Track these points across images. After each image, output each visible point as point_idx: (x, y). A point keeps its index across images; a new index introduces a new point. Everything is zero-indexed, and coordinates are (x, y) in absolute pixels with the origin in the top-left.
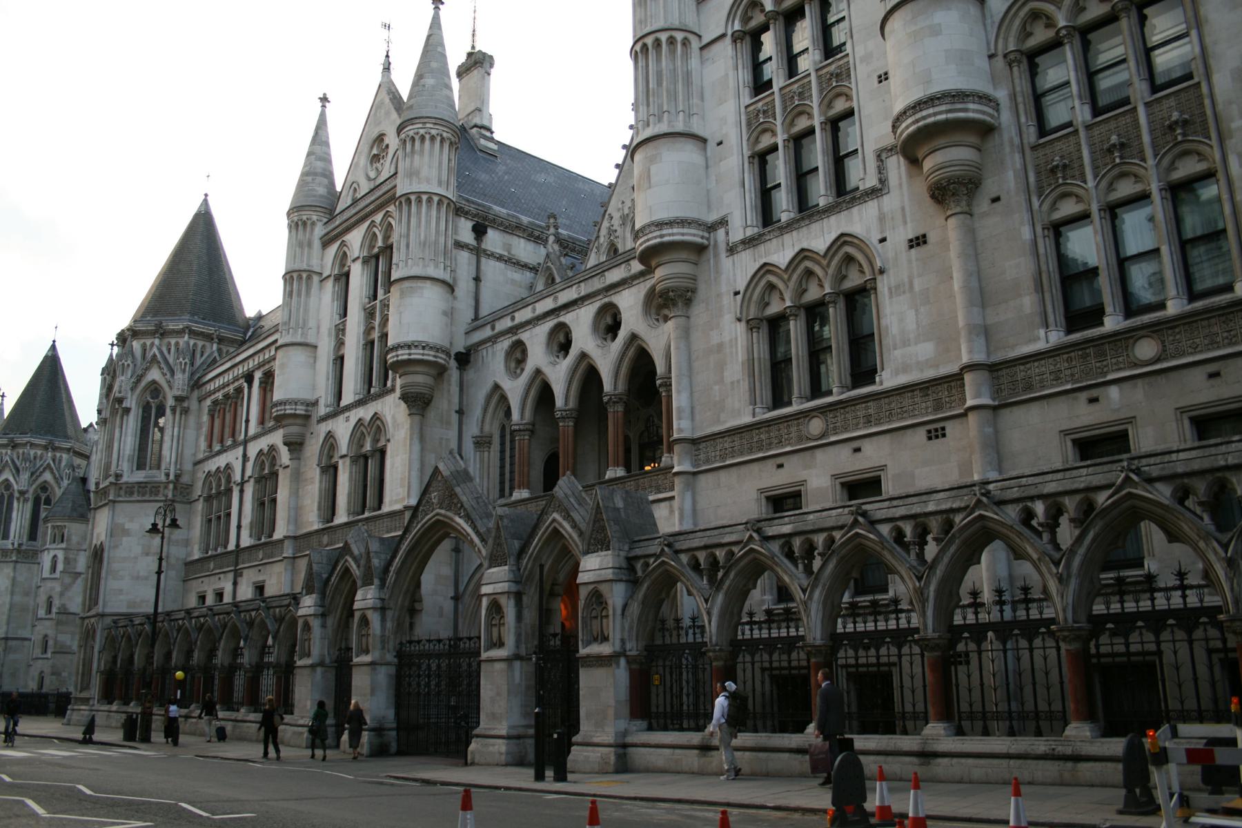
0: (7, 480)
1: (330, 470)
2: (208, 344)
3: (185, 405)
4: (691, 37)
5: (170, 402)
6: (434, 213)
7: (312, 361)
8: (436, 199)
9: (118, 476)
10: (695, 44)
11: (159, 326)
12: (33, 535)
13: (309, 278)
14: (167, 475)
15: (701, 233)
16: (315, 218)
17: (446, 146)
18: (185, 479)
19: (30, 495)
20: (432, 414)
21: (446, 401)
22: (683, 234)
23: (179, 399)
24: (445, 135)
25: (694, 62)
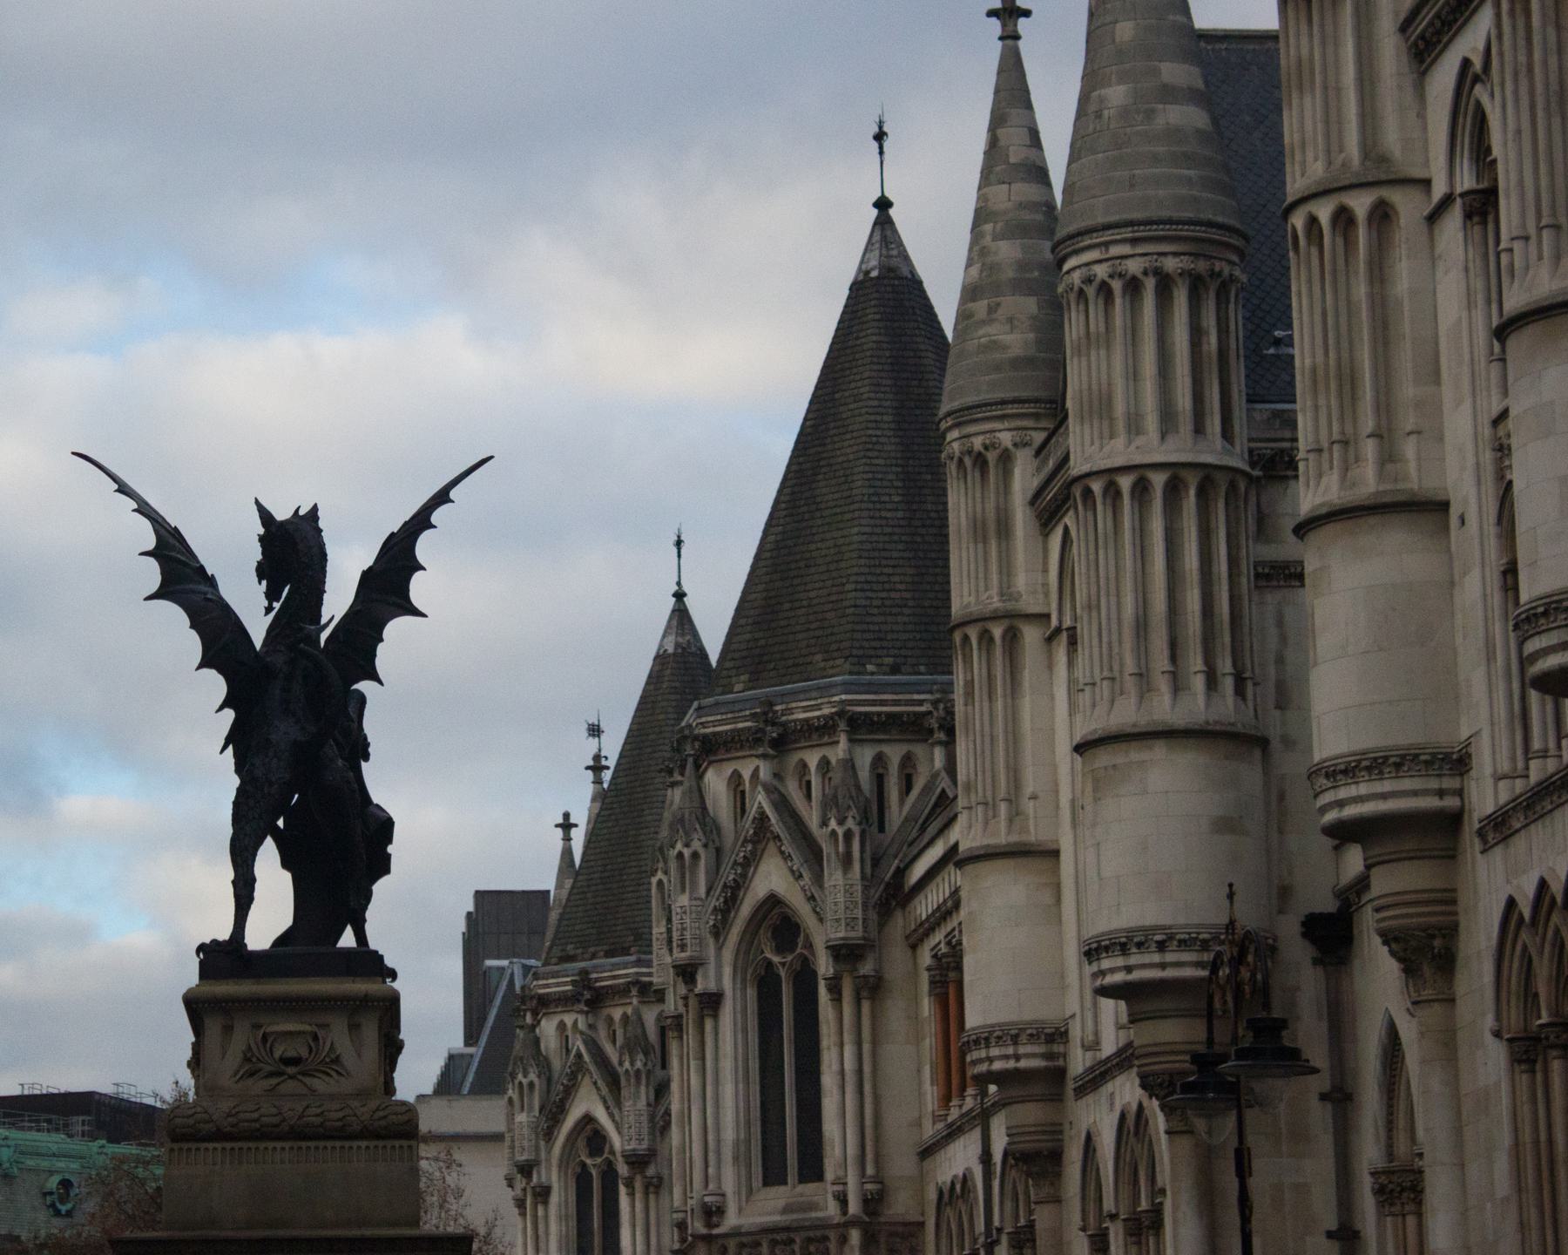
0: (588, 1119)
2: (919, 750)
3: (867, 968)
4: (1396, 196)
5: (824, 965)
6: (1157, 525)
7: (1047, 897)
8: (1158, 480)
9: (712, 1213)
10: (1409, 208)
11: (767, 715)
13: (1012, 637)
14: (842, 1200)
15: (1434, 784)
16: (1006, 438)
17: (1181, 298)
18: (900, 1206)
22: (1384, 796)
23: (846, 954)
24: (1170, 264)
25: (1404, 274)
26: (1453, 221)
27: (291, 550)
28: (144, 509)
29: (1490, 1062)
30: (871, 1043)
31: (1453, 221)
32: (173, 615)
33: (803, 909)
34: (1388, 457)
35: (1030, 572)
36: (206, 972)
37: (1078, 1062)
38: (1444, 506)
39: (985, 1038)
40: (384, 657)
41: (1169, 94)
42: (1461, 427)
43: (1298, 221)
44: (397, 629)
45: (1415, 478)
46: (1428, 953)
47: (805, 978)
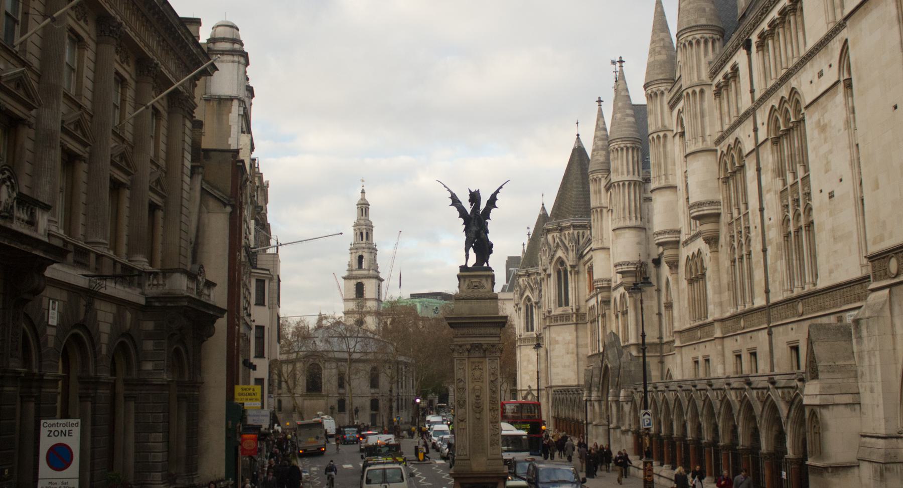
4: (668, 133)
5: (569, 269)
10: (670, 135)
23: (573, 267)
25: (669, 147)
26: (677, 137)
27: (475, 197)
28: (449, 190)
29: (684, 284)
30: (577, 282)
31: (677, 137)
32: (454, 209)
33: (565, 259)
34: (667, 179)
36: (461, 271)
37: (613, 285)
38: (676, 187)
39: (597, 281)
40: (491, 215)
41: (628, 115)
42: (679, 173)
43: (650, 137)
44: (493, 211)
45: (671, 182)
46: (674, 265)
47: (566, 271)
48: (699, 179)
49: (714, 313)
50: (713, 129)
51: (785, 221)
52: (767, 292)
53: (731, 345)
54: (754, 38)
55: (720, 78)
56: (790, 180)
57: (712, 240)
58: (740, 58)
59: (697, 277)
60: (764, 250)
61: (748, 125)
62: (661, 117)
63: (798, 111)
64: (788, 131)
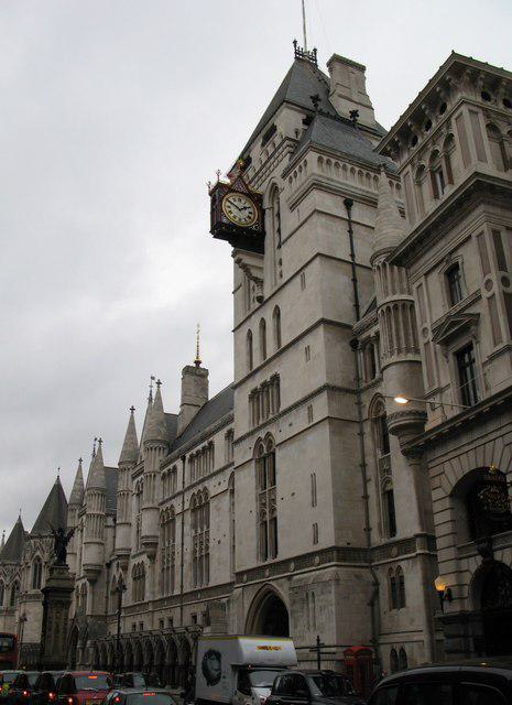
1: (78, 597)
12: (12, 604)
19: (10, 587)
20: (97, 584)
21: (102, 580)
35: (77, 522)
46: (125, 569)
48: (150, 523)
49: (148, 597)
50: (159, 497)
51: (195, 552)
52: (182, 587)
53: (157, 616)
54: (188, 456)
55: (165, 470)
56: (199, 531)
57: (152, 557)
58: (179, 463)
59: (140, 576)
60: (182, 566)
61: (179, 499)
62: (126, 483)
63: (206, 497)
64: (200, 507)
